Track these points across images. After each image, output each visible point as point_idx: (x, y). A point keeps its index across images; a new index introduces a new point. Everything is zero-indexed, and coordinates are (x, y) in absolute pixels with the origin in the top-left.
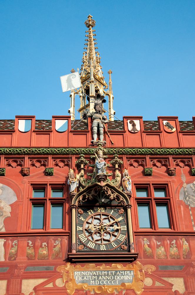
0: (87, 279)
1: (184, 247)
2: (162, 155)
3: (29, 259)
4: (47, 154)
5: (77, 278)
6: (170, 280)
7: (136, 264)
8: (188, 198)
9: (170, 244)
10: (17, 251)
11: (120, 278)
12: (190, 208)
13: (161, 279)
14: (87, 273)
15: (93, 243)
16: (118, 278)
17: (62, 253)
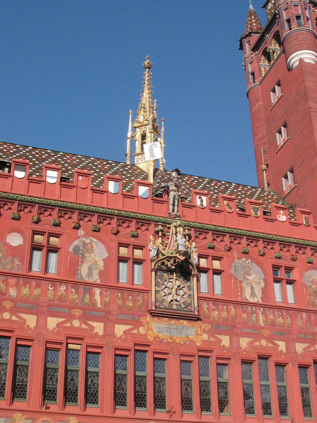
1: (232, 312)
3: (119, 308)
6: (220, 337)
8: (237, 272)
9: (222, 308)
10: (110, 300)
12: (238, 281)
16: (184, 331)
17: (144, 307)
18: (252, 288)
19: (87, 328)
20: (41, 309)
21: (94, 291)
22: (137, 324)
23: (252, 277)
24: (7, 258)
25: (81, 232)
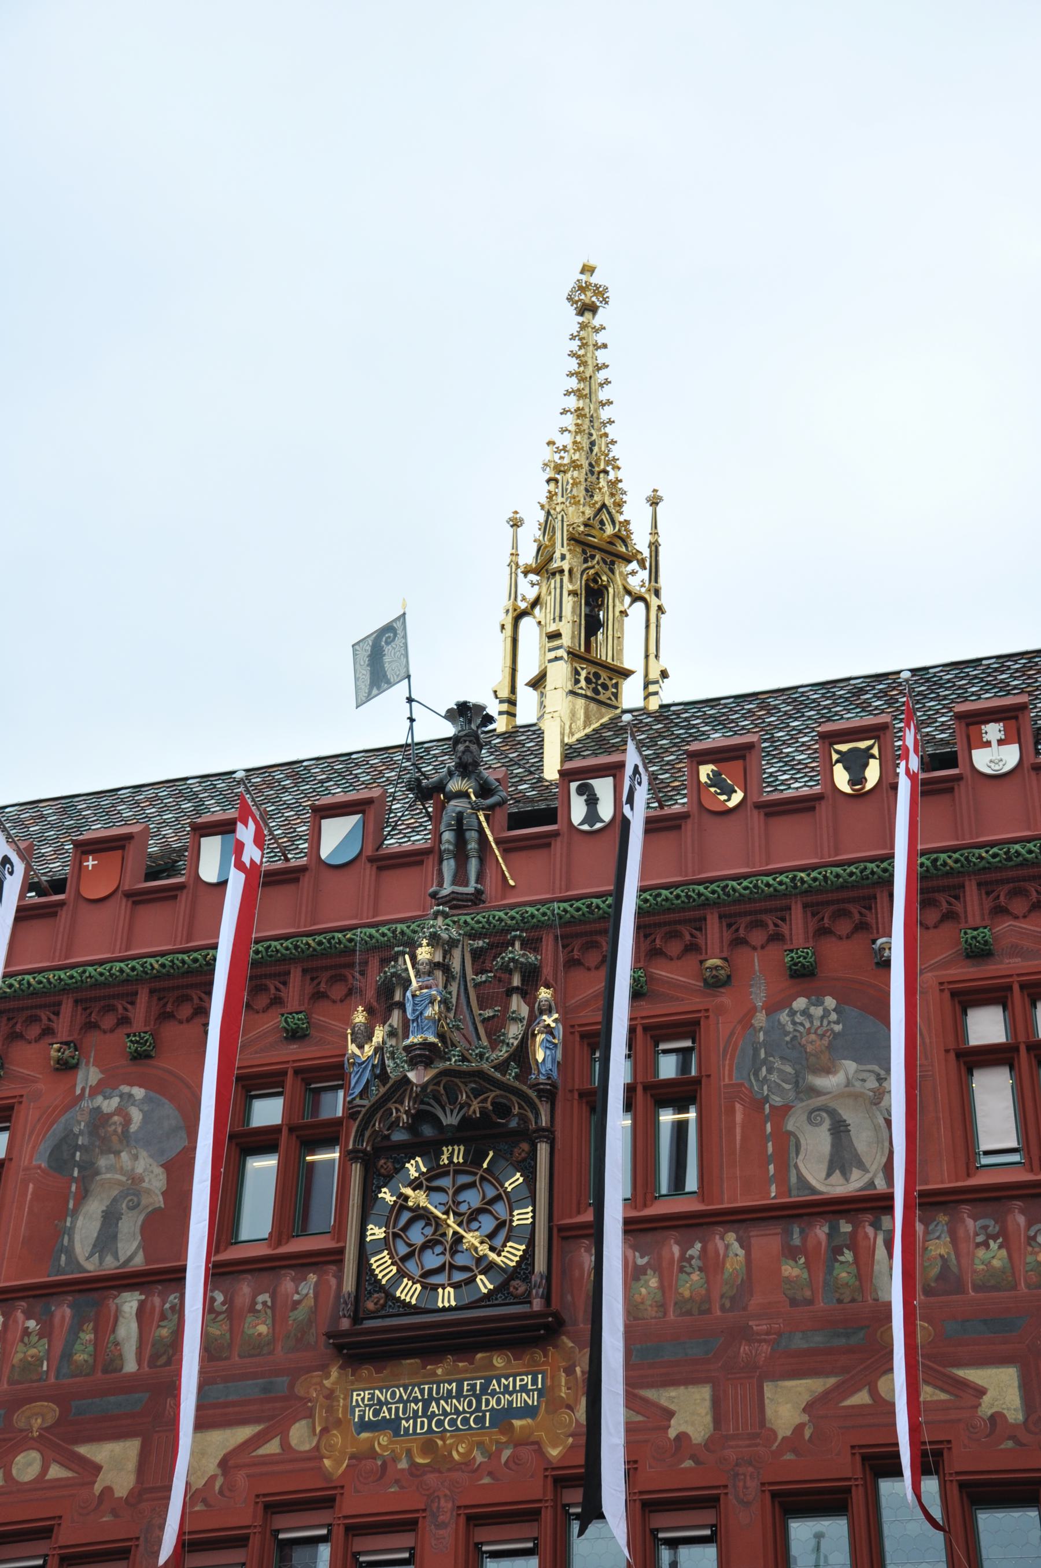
0: (390, 1414)
1: (728, 1265)
2: (683, 910)
4: (284, 959)
5: (357, 1413)
7: (555, 1347)
8: (764, 1069)
9: (682, 1258)
11: (498, 1402)
14: (393, 1394)
15: (414, 1283)
16: (493, 1402)
18: (840, 1130)
21: (117, 1305)
25: (89, 1075)
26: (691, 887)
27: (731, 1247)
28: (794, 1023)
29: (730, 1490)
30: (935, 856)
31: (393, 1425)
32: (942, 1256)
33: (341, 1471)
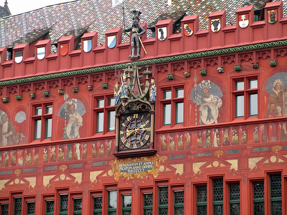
2: (179, 61)
3: (93, 157)
6: (175, 166)
9: (179, 138)
10: (87, 152)
13: (170, 166)
14: (126, 165)
16: (144, 167)
18: (209, 110)
19: (70, 179)
20: (37, 171)
22: (106, 168)
23: (210, 98)
24: (16, 135)
25: (66, 96)
26: (181, 56)
27: (188, 135)
28: (202, 86)
29: (186, 184)
30: (229, 49)
31: (126, 171)
32: (226, 137)
33: (118, 180)
